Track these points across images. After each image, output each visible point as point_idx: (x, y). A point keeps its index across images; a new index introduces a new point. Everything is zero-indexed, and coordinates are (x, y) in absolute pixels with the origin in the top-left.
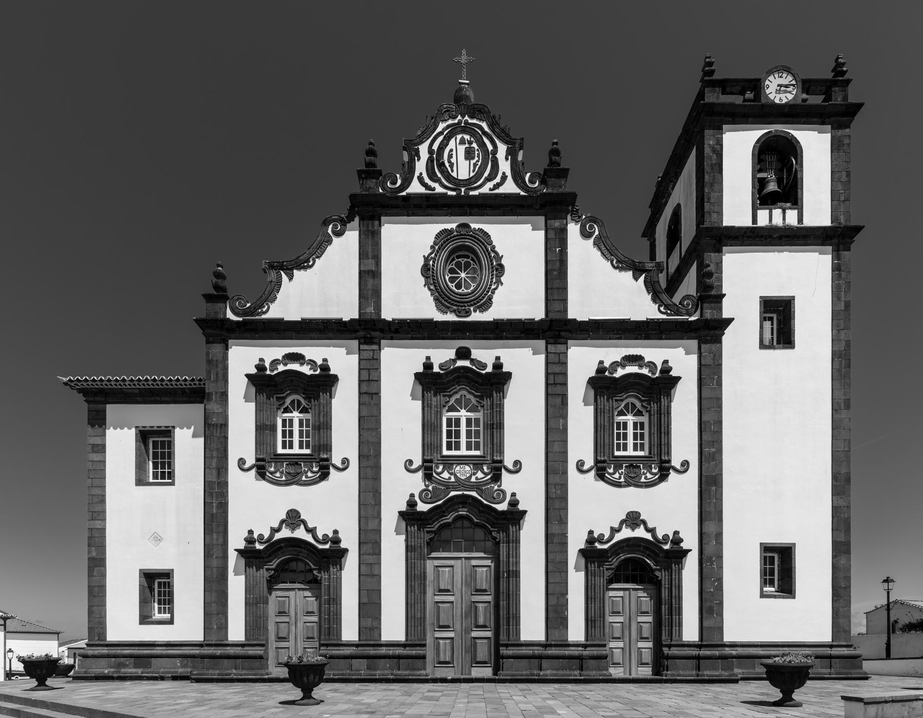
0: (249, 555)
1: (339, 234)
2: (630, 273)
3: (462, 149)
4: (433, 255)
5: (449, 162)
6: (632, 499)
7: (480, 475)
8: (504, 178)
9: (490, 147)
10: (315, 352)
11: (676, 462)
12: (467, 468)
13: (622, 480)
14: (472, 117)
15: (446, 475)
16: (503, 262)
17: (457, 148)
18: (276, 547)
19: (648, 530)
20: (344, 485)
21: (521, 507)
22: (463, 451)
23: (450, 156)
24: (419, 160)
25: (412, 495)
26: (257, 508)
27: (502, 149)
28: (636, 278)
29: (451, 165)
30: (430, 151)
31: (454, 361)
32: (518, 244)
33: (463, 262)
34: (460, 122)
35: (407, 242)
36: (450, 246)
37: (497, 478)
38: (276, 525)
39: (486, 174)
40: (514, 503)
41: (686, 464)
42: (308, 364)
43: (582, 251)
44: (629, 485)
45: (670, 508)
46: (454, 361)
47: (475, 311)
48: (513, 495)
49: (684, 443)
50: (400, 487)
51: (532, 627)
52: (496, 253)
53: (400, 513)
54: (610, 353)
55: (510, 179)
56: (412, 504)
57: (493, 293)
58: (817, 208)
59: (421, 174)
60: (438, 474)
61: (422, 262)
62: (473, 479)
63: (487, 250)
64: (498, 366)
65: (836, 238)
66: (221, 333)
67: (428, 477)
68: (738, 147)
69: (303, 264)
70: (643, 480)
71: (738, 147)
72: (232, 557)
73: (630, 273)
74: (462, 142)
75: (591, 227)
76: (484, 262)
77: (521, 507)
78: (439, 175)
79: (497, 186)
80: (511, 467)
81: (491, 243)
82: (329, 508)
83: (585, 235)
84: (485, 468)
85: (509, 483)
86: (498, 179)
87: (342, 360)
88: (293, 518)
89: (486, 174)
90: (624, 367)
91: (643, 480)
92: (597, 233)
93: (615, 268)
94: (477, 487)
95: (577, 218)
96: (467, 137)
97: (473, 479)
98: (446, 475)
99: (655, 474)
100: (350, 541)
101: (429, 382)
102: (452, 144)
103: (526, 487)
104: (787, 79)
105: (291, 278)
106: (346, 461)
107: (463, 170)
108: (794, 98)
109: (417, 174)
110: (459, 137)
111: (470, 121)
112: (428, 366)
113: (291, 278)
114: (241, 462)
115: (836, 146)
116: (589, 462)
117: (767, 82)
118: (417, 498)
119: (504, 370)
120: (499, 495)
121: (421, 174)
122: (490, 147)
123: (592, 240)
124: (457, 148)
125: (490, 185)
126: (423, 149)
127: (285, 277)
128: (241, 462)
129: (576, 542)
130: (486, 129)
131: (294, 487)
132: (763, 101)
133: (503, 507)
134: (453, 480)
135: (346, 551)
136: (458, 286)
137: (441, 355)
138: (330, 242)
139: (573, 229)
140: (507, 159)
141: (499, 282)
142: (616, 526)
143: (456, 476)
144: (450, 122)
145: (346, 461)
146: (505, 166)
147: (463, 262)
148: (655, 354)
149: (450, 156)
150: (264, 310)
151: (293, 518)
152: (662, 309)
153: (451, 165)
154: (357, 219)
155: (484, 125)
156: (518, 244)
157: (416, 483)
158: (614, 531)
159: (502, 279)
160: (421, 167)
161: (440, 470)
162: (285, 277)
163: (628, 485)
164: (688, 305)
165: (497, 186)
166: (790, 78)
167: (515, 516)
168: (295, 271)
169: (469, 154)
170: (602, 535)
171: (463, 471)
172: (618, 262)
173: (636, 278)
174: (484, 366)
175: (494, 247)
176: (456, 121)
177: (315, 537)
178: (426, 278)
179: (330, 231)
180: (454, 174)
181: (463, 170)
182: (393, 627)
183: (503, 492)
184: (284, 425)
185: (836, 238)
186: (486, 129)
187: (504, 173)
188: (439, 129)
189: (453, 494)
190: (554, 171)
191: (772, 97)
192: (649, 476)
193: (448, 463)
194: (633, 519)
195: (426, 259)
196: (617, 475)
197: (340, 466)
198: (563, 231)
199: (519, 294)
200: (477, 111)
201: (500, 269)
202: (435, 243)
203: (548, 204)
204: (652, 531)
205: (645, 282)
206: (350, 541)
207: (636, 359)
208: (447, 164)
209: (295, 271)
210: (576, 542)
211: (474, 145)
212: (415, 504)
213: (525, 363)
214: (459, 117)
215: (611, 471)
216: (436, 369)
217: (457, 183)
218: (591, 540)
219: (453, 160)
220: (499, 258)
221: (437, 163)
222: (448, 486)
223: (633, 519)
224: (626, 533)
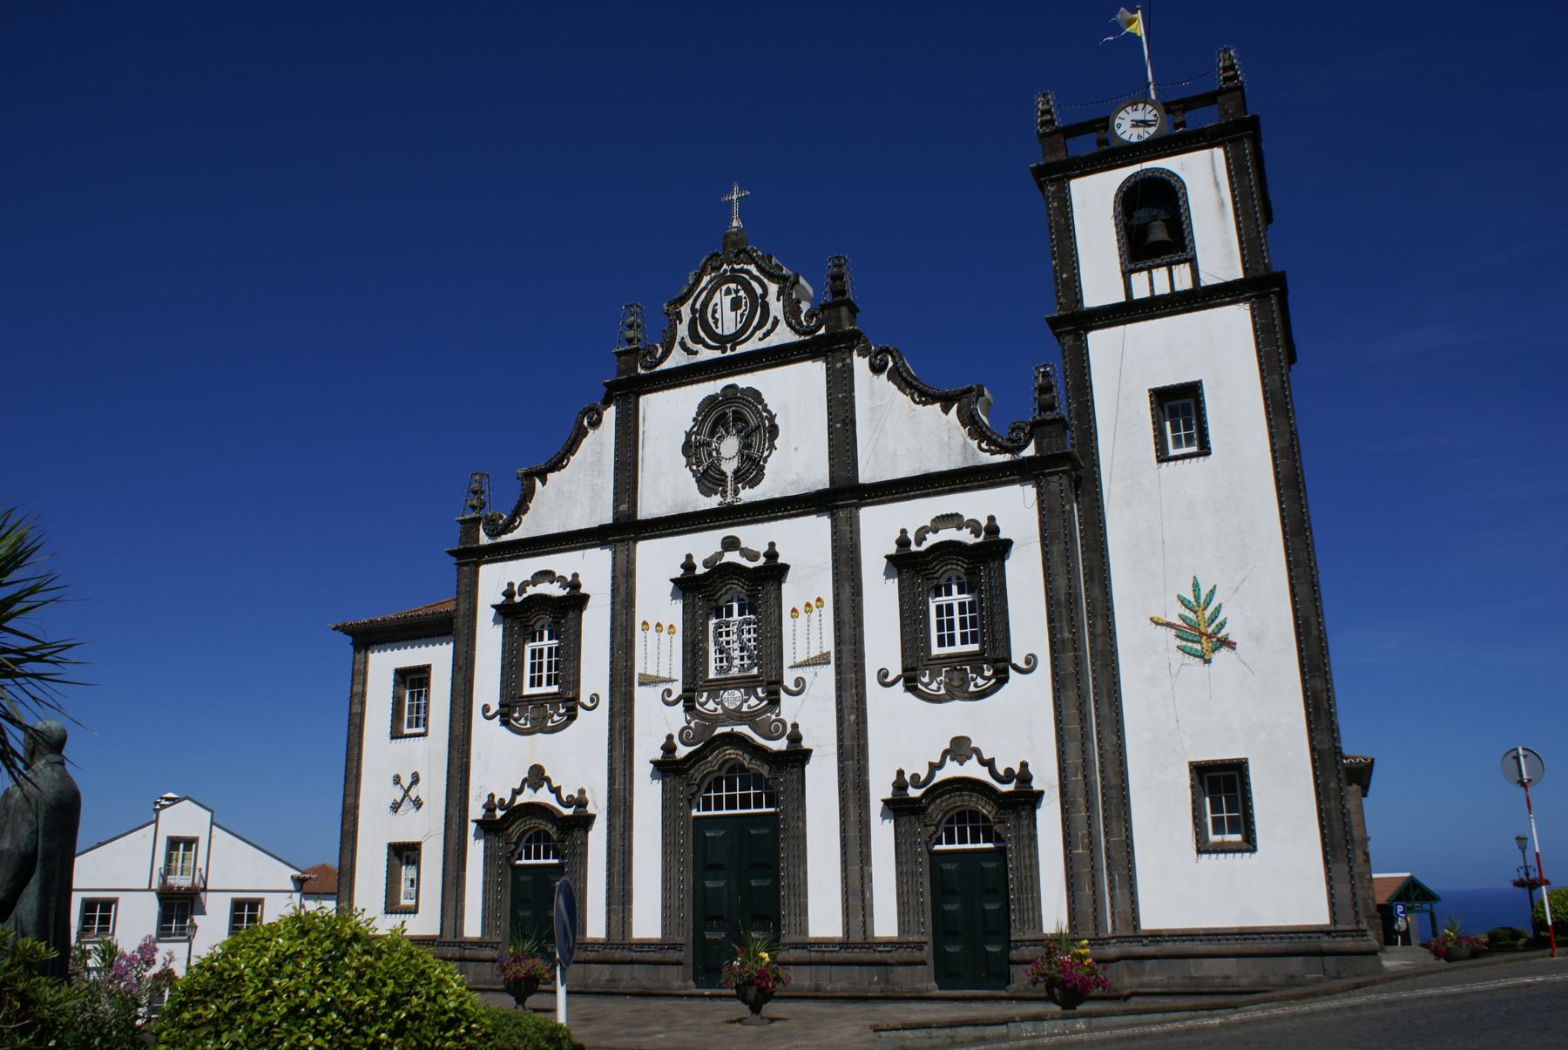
0: (488, 827)
3: (727, 300)
6: (958, 717)
7: (753, 701)
8: (776, 322)
9: (759, 291)
10: (563, 563)
11: (1018, 658)
12: (737, 694)
13: (943, 691)
15: (711, 705)
17: (722, 301)
18: (517, 812)
19: (983, 762)
20: (593, 726)
21: (805, 744)
22: (734, 672)
23: (714, 311)
25: (670, 737)
26: (501, 762)
27: (773, 288)
28: (946, 410)
29: (716, 323)
30: (693, 310)
31: (720, 555)
32: (794, 393)
35: (668, 415)
37: (774, 702)
38: (517, 786)
39: (755, 323)
40: (795, 738)
41: (1031, 661)
43: (873, 391)
44: (953, 698)
45: (1016, 727)
46: (720, 555)
48: (795, 726)
49: (1028, 629)
50: (658, 722)
51: (824, 918)
52: (769, 412)
53: (655, 763)
54: (915, 514)
56: (669, 748)
60: (702, 705)
62: (745, 709)
64: (772, 554)
66: (471, 557)
67: (690, 708)
69: (557, 465)
70: (972, 689)
72: (472, 827)
74: (728, 292)
77: (805, 744)
78: (702, 334)
80: (792, 687)
81: (761, 401)
82: (575, 759)
83: (876, 369)
84: (759, 690)
85: (789, 708)
86: (768, 326)
87: (592, 568)
88: (537, 777)
89: (755, 323)
90: (936, 532)
91: (972, 689)
92: (891, 364)
94: (750, 718)
96: (733, 286)
97: (745, 709)
98: (711, 705)
99: (988, 679)
100: (598, 805)
101: (688, 585)
102: (716, 298)
103: (811, 712)
106: (595, 698)
107: (728, 322)
109: (678, 340)
110: (724, 288)
112: (689, 566)
114: (486, 708)
116: (895, 670)
118: (676, 740)
119: (780, 561)
120: (777, 728)
122: (759, 291)
123: (884, 376)
124: (722, 301)
125: (759, 334)
126: (685, 310)
127: (538, 482)
128: (486, 708)
129: (880, 789)
131: (539, 735)
133: (780, 745)
134: (720, 711)
135: (593, 817)
137: (703, 546)
138: (585, 434)
139: (861, 364)
141: (772, 447)
142: (937, 760)
143: (723, 707)
145: (595, 698)
146: (776, 308)
148: (975, 504)
149: (714, 311)
151: (537, 777)
152: (984, 445)
153: (716, 323)
155: (752, 268)
156: (794, 393)
157: (676, 718)
158: (934, 768)
160: (683, 330)
161: (703, 700)
162: (538, 482)
163: (950, 696)
167: (798, 757)
169: (736, 304)
170: (915, 777)
171: (732, 698)
173: (946, 410)
174: (753, 556)
177: (559, 799)
180: (719, 331)
182: (647, 922)
183: (783, 723)
184: (533, 657)
188: (703, 284)
189: (720, 730)
190: (836, 301)
192: (980, 681)
193: (716, 688)
194: (960, 749)
196: (934, 686)
197: (589, 705)
198: (849, 370)
199: (798, 461)
201: (774, 431)
202: (698, 414)
203: (827, 344)
204: (989, 764)
206: (598, 805)
207: (953, 520)
208: (711, 321)
210: (880, 789)
211: (742, 293)
212: (675, 749)
213: (804, 544)
215: (926, 680)
216: (700, 570)
217: (722, 341)
218: (900, 785)
219: (718, 316)
220: (772, 417)
221: (700, 318)
222: (715, 720)
223: (960, 749)
224: (952, 770)
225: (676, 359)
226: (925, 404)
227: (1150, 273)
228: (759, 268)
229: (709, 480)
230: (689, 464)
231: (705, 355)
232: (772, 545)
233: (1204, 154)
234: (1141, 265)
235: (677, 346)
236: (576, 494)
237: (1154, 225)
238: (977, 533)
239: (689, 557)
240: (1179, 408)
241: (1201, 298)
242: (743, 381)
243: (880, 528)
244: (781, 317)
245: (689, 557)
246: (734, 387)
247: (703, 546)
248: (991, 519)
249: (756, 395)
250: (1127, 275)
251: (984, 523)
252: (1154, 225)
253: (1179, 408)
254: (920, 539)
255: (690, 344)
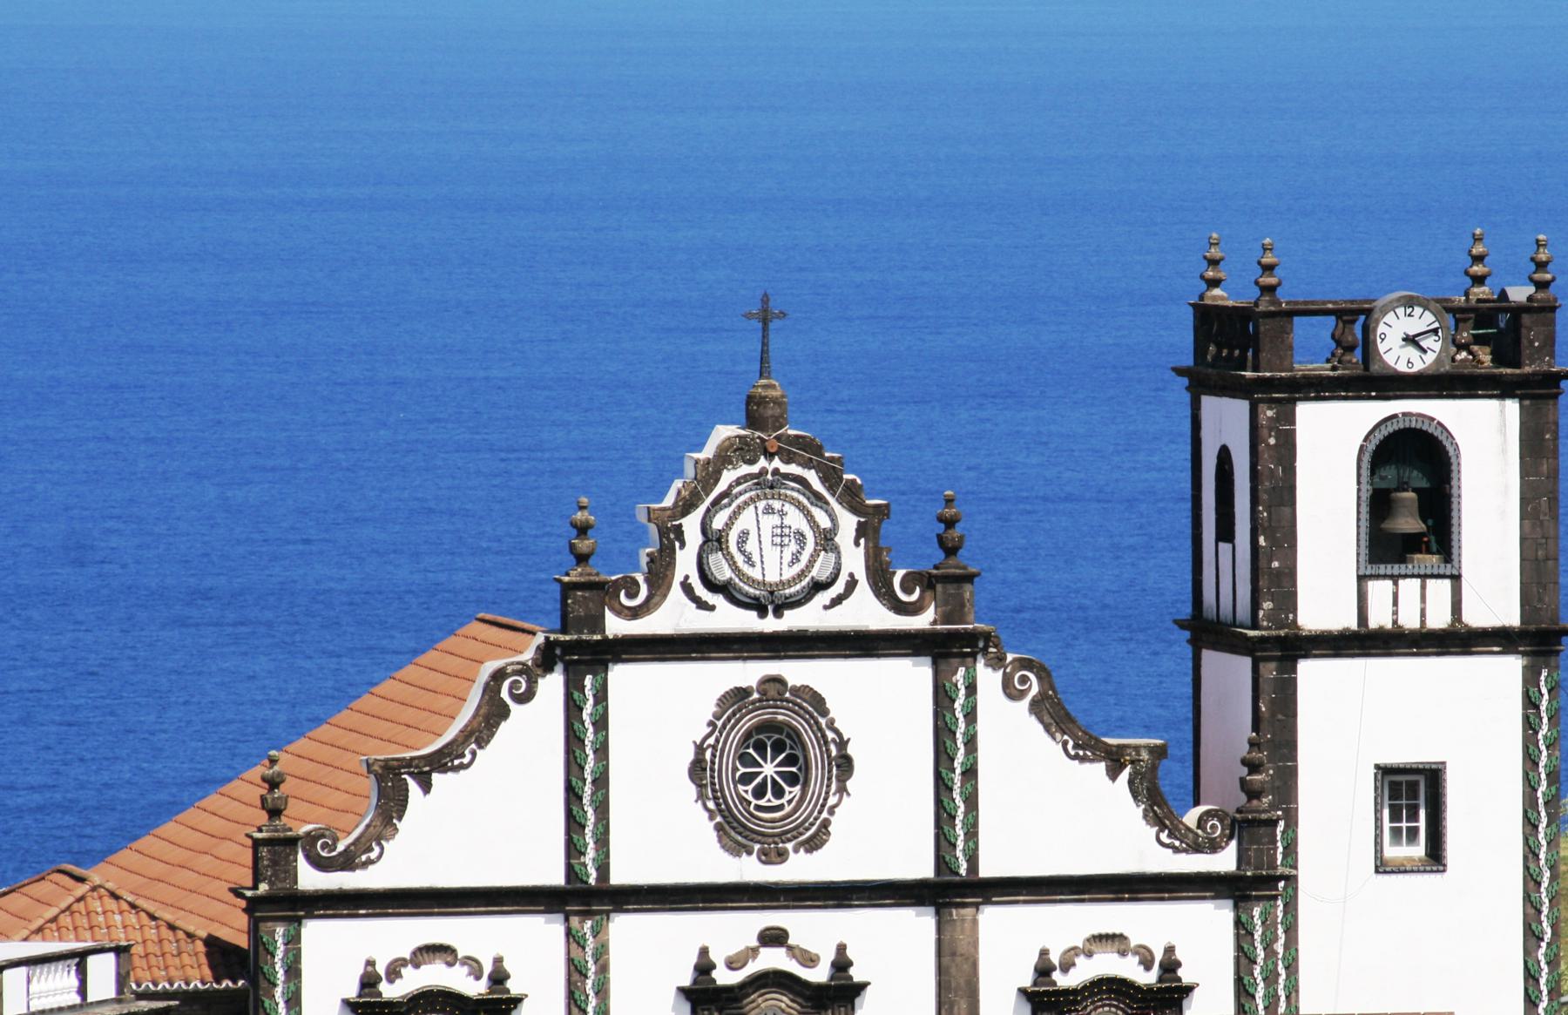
1: (525, 698)
2: (1101, 767)
4: (711, 741)
5: (743, 552)
8: (852, 584)
10: (476, 935)
14: (787, 462)
16: (851, 750)
24: (683, 545)
27: (848, 522)
28: (1113, 774)
29: (749, 560)
33: (773, 758)
34: (763, 472)
35: (661, 714)
36: (747, 723)
42: (463, 964)
43: (1006, 726)
47: (796, 851)
52: (836, 731)
54: (1062, 926)
55: (864, 588)
57: (832, 811)
58: (1491, 583)
59: (687, 577)
61: (690, 755)
63: (820, 729)
65: (1534, 640)
68: (1331, 442)
71: (1331, 442)
73: (1101, 767)
75: (1024, 680)
76: (814, 752)
79: (837, 601)
81: (824, 712)
83: (1011, 692)
90: (1089, 955)
92: (1035, 689)
93: (1076, 757)
95: (997, 662)
104: (1421, 320)
105: (426, 787)
108: (1438, 361)
109: (678, 578)
111: (784, 469)
113: (426, 787)
115: (1536, 447)
117: (1381, 328)
121: (687, 577)
126: (691, 525)
127: (413, 787)
130: (817, 486)
132: (1375, 368)
136: (759, 792)
138: (504, 713)
139: (988, 679)
140: (857, 544)
144: (745, 469)
147: (773, 758)
150: (373, 855)
152: (1164, 837)
154: (559, 668)
155: (812, 477)
156: (879, 708)
159: (849, 784)
162: (413, 787)
164: (1213, 827)
165: (837, 601)
166: (1429, 317)
168: (435, 777)
172: (1076, 746)
173: (1113, 774)
174: (810, 960)
175: (832, 721)
176: (755, 469)
178: (701, 786)
179: (504, 694)
181: (773, 566)
185: (1534, 640)
186: (817, 486)
187: (851, 575)
188: (722, 486)
191: (1390, 359)
195: (700, 749)
200: (804, 450)
205: (1131, 782)
209: (435, 777)
214: (762, 462)
220: (842, 744)
225: (674, 616)
226: (1083, 759)
227: (1396, 584)
228: (824, 480)
229: (734, 831)
230: (701, 797)
231: (729, 618)
232: (841, 949)
233: (1491, 405)
234: (1382, 569)
235: (676, 591)
236: (489, 816)
237: (1410, 501)
238: (1147, 964)
239: (704, 952)
240: (1413, 794)
241: (1458, 640)
242: (796, 672)
243: (1010, 943)
244: (861, 575)
245: (704, 952)
246: (778, 680)
247: (729, 935)
248: (1170, 950)
249: (818, 702)
250: (1362, 579)
251: (1159, 956)
252: (1410, 501)
253: (1413, 794)
254: (1066, 967)
255: (701, 591)
